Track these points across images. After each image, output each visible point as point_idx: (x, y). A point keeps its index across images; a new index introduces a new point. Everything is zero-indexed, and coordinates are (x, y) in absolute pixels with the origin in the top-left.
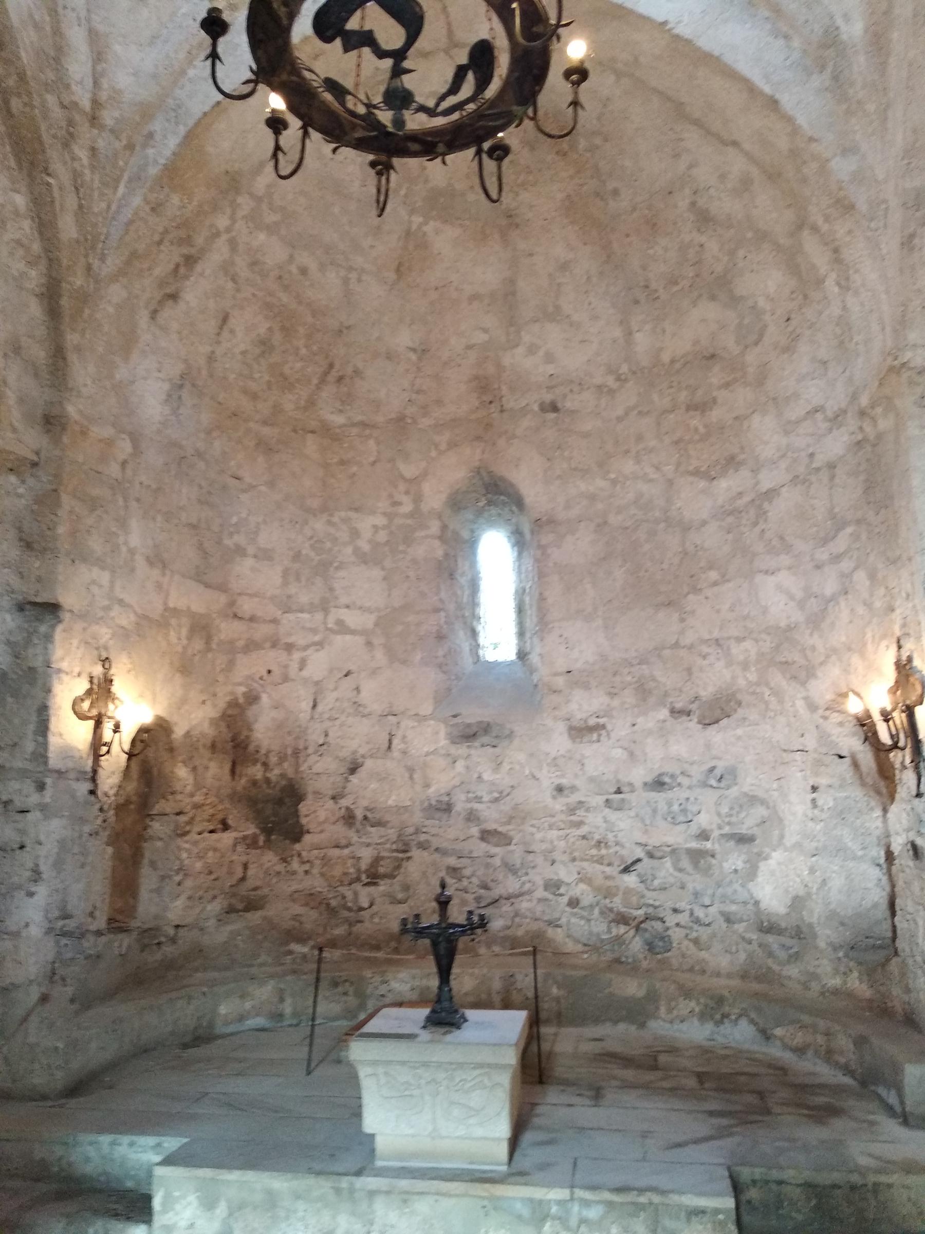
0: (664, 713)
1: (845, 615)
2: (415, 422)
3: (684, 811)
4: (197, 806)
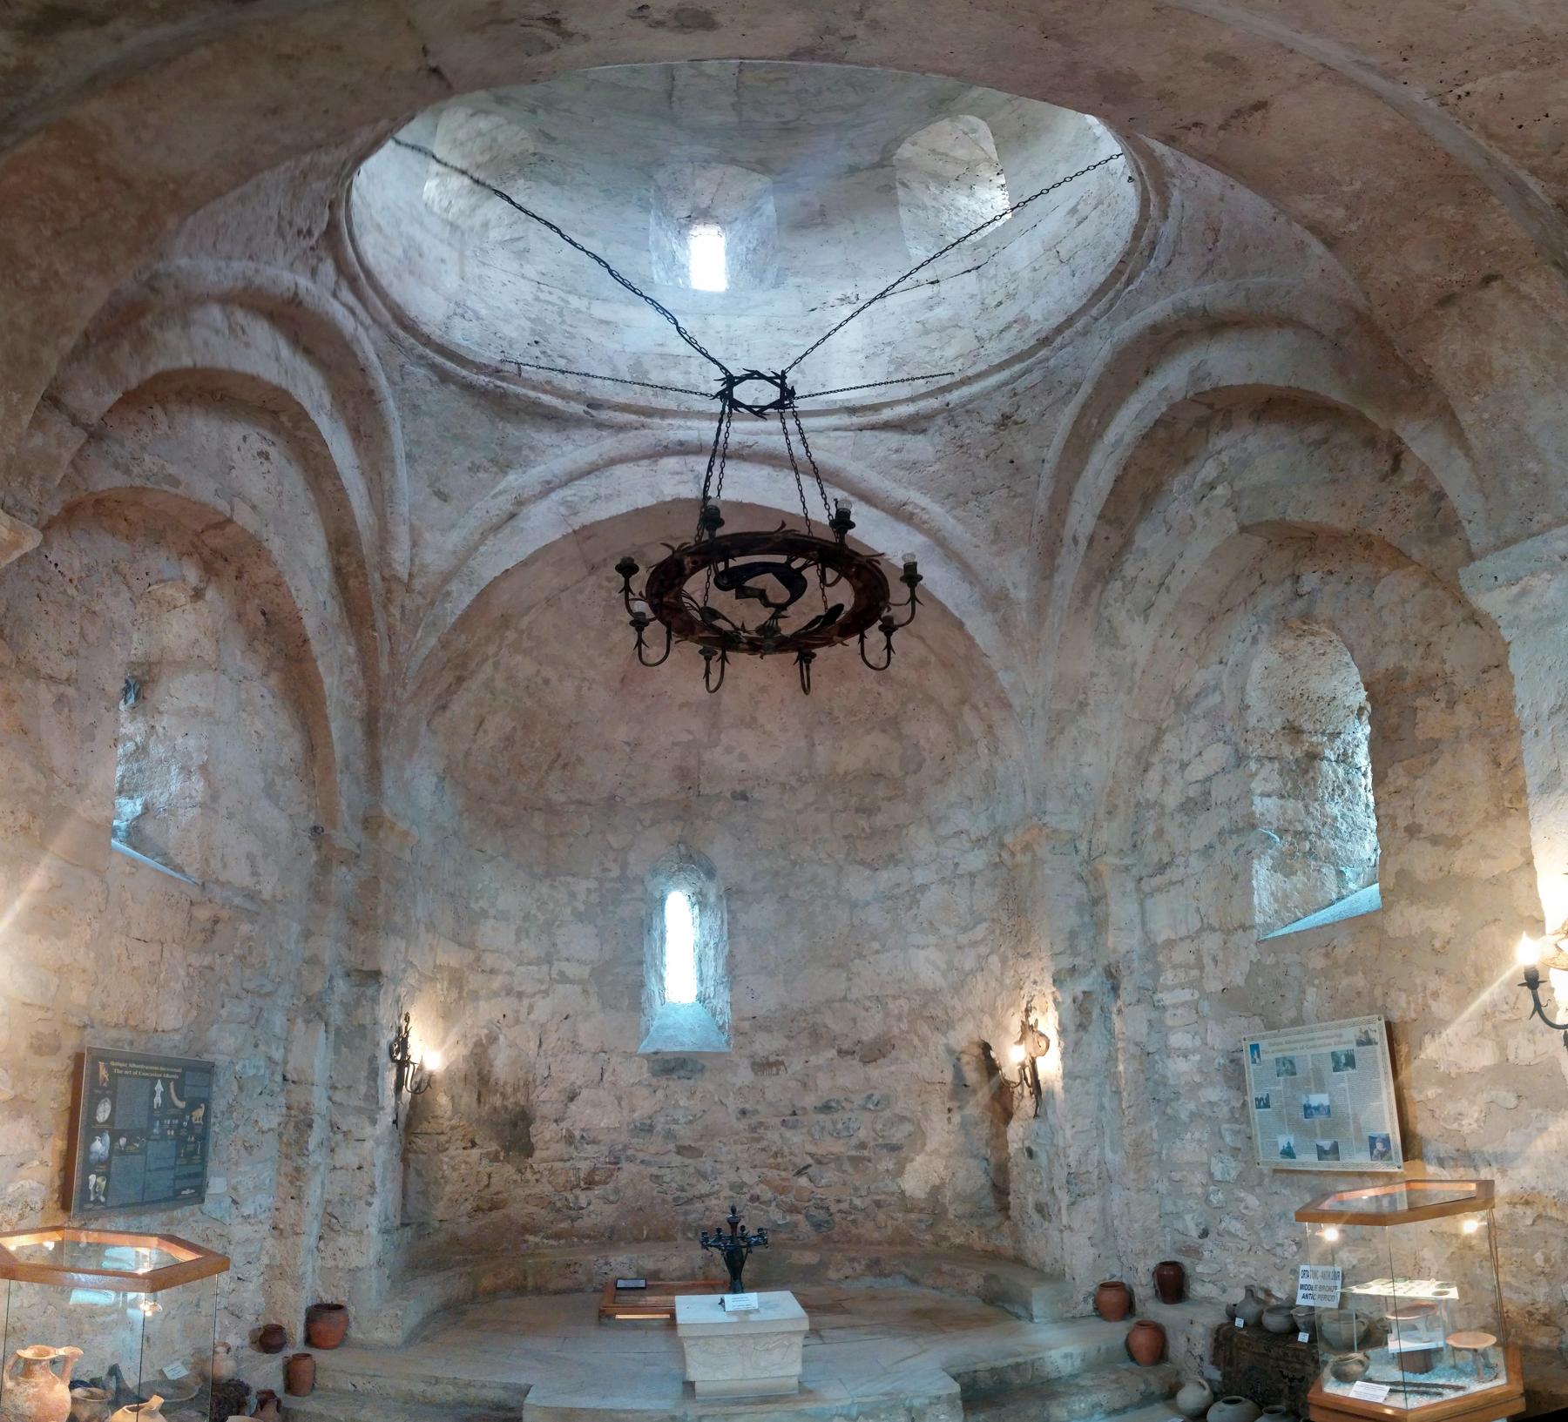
0: (832, 1053)
1: (981, 986)
2: (623, 800)
3: (848, 1128)
4: (453, 1128)
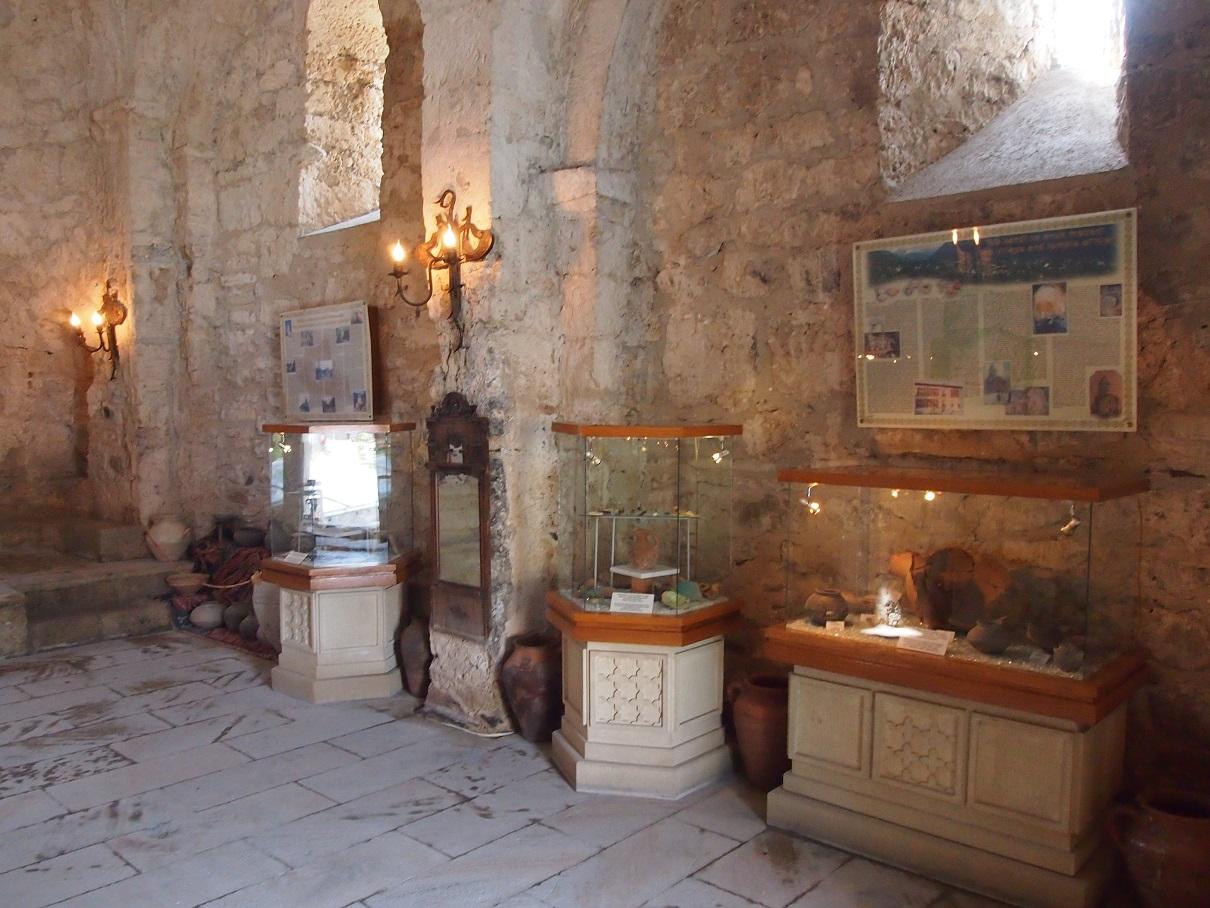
1: (65, 256)
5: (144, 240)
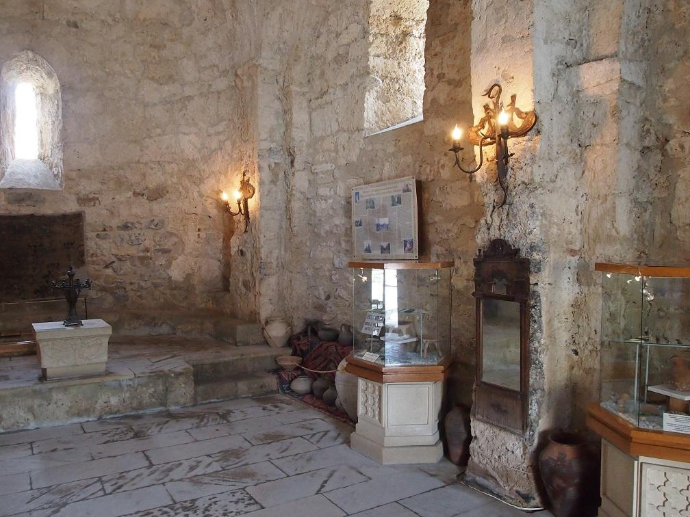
0: (130, 194)
1: (220, 159)
5: (265, 145)
